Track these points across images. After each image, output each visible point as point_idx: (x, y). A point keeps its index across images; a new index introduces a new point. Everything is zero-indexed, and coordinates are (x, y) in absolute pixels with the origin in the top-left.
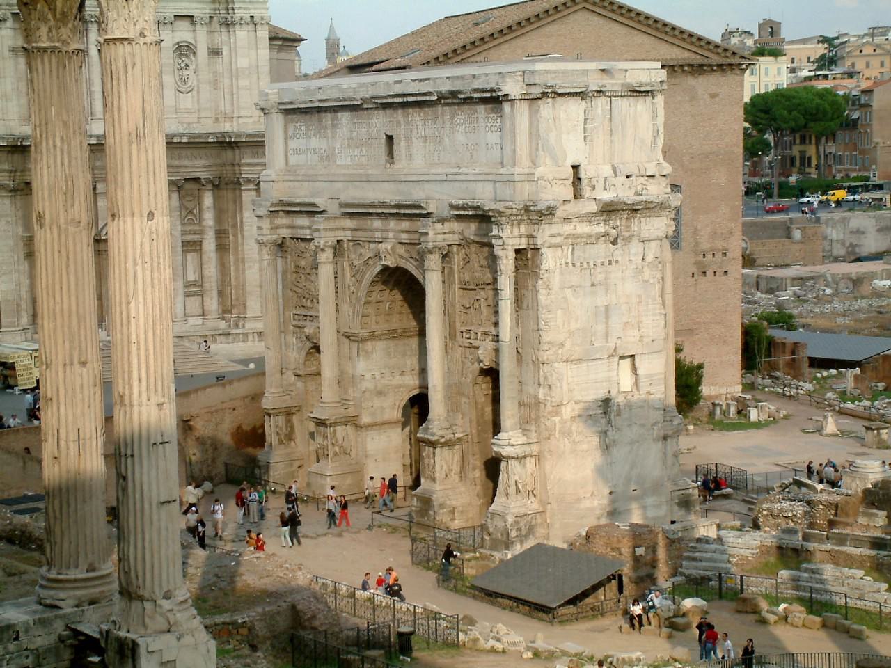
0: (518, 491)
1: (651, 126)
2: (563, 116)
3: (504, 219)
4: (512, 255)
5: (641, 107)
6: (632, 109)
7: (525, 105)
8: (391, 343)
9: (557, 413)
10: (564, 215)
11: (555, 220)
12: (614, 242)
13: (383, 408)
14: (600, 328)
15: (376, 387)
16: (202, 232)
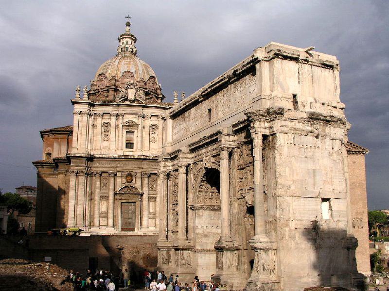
0: (264, 269)
1: (333, 85)
2: (287, 69)
3: (256, 117)
4: (261, 138)
5: (327, 72)
6: (323, 74)
7: (267, 64)
8: (212, 213)
9: (287, 225)
10: (289, 117)
11: (284, 118)
12: (317, 137)
13: (207, 243)
14: (310, 181)
15: (204, 232)
16: (156, 194)
